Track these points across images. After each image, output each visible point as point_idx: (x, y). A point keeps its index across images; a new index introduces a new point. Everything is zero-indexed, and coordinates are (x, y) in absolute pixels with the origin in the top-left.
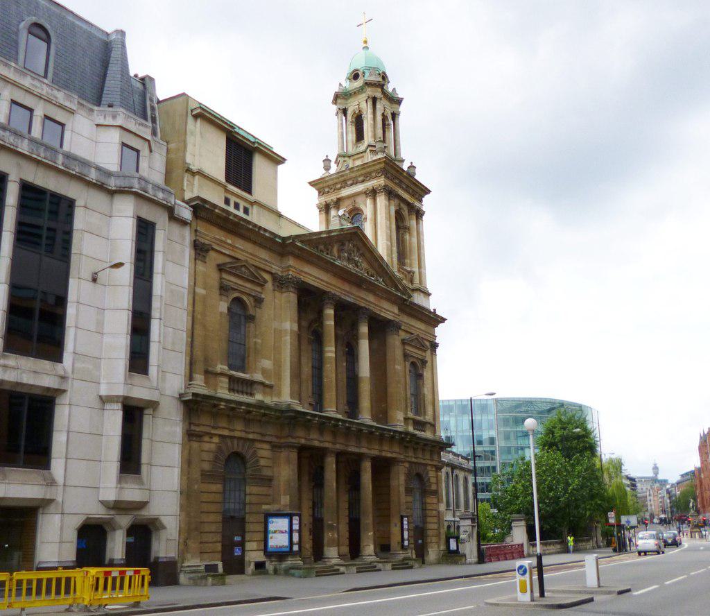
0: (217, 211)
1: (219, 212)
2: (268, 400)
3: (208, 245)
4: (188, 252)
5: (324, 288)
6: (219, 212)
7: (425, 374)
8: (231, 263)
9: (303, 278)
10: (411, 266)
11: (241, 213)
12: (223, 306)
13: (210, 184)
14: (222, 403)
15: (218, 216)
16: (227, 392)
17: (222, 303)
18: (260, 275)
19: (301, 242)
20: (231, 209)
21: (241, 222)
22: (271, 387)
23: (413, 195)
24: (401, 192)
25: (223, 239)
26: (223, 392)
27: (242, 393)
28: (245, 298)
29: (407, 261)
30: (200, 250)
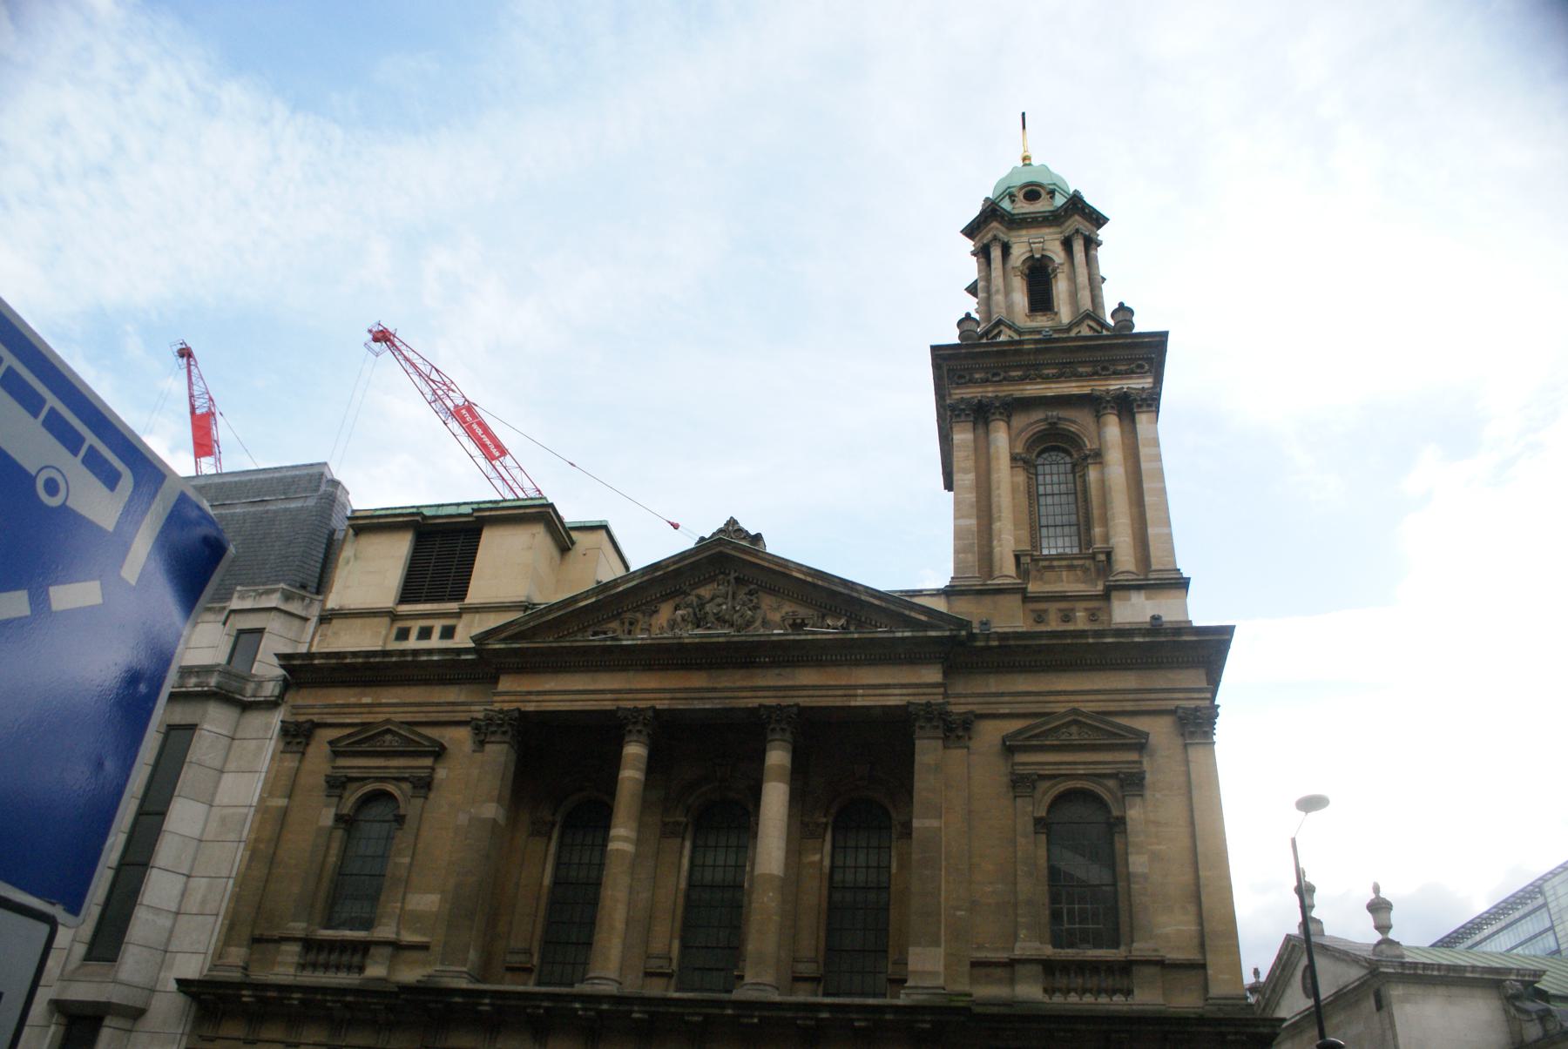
0: (316, 662)
1: (322, 661)
2: (410, 974)
3: (307, 722)
4: (271, 745)
5: (609, 706)
6: (322, 661)
7: (1134, 813)
8: (349, 735)
9: (531, 707)
10: (1106, 538)
11: (435, 642)
12: (327, 817)
13: (359, 622)
14: (244, 992)
15: (333, 669)
16: (292, 971)
17: (324, 811)
18: (419, 735)
19: (504, 640)
20: (412, 643)
21: (372, 660)
22: (424, 947)
23: (1104, 369)
24: (1032, 390)
25: (353, 700)
26: (284, 969)
27: (326, 967)
28: (390, 788)
29: (1097, 531)
30: (296, 736)
